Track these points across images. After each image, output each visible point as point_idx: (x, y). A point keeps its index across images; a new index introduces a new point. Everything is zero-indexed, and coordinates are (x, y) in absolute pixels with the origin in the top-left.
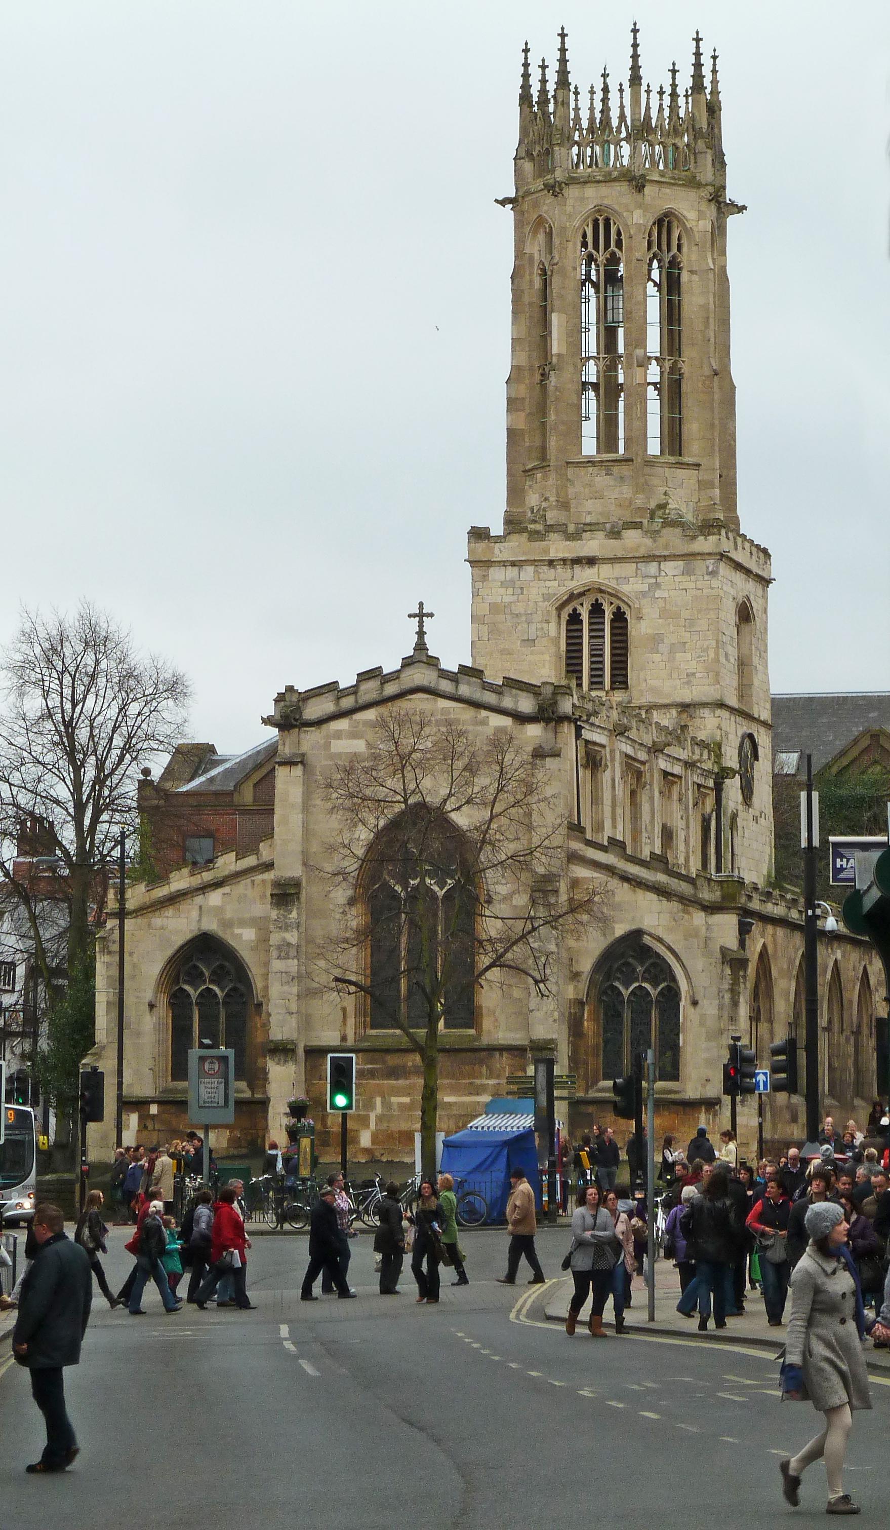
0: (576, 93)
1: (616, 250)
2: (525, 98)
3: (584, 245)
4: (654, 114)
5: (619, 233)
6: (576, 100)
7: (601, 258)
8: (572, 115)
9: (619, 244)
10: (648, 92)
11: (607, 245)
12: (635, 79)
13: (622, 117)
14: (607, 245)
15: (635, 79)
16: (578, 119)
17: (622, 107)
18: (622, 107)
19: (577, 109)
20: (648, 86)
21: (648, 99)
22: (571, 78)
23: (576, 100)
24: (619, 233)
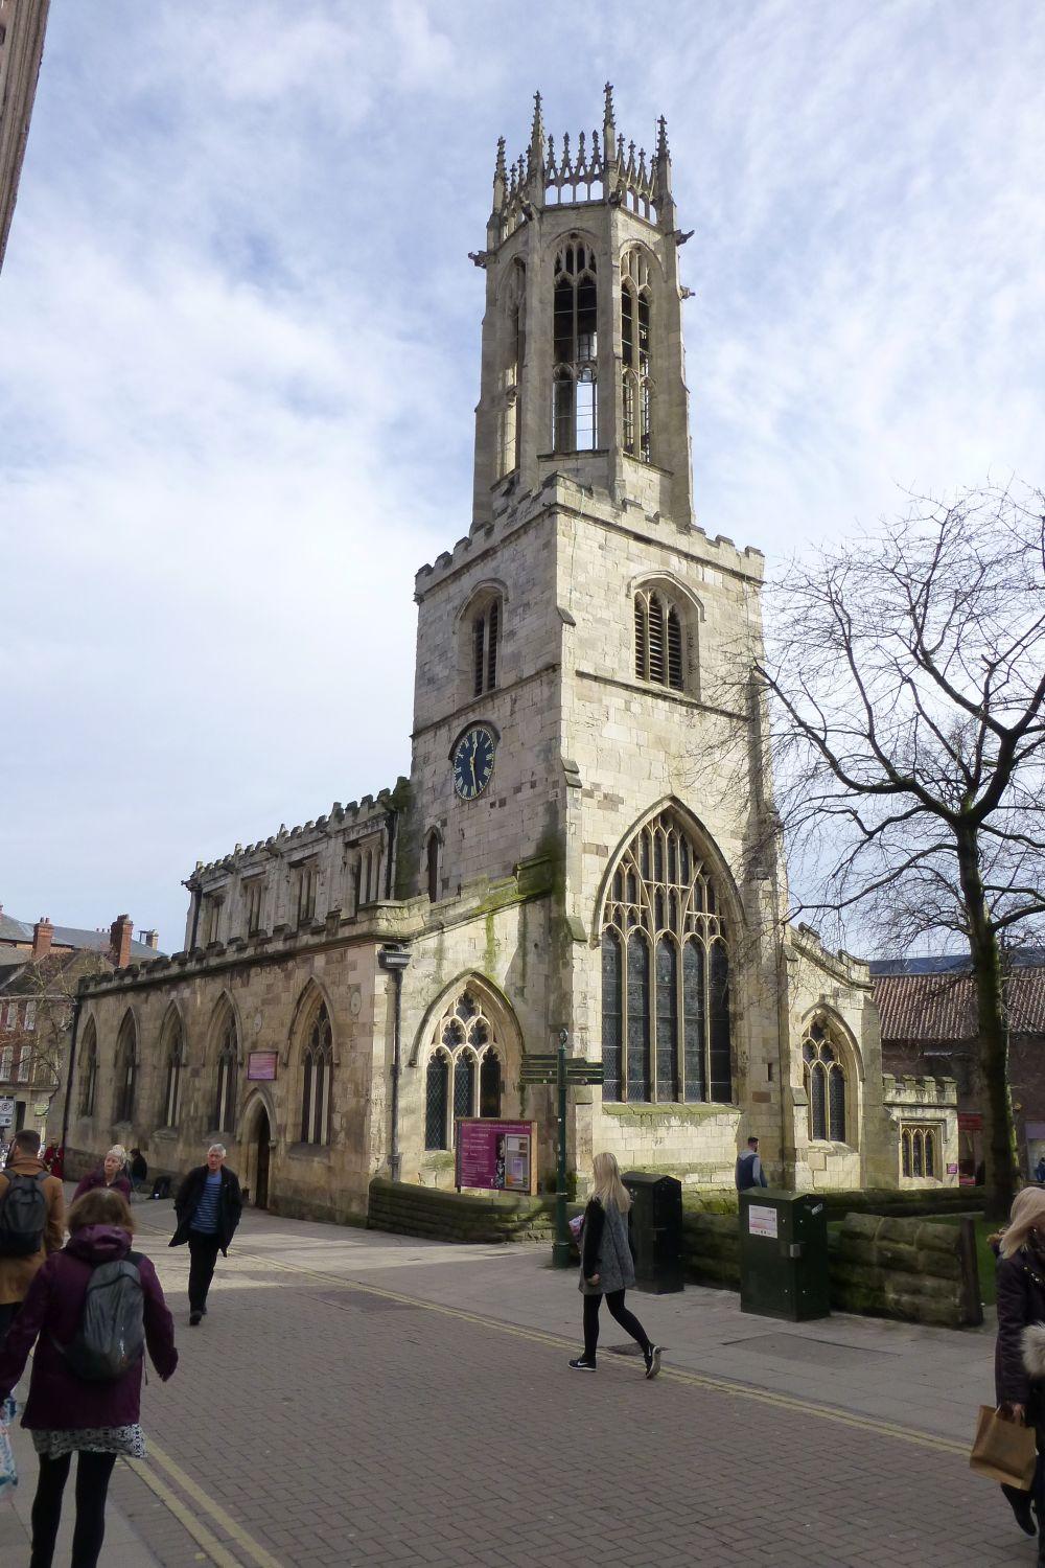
0: (551, 139)
1: (590, 272)
2: (500, 177)
3: (558, 270)
4: (626, 159)
5: (592, 258)
6: (551, 146)
7: (575, 279)
8: (546, 158)
9: (593, 267)
10: (621, 140)
11: (581, 266)
12: (609, 122)
13: (596, 158)
14: (581, 266)
15: (609, 122)
16: (552, 163)
17: (596, 149)
18: (596, 149)
19: (551, 154)
20: (621, 135)
21: (621, 145)
22: (546, 134)
23: (551, 146)
24: (592, 258)
